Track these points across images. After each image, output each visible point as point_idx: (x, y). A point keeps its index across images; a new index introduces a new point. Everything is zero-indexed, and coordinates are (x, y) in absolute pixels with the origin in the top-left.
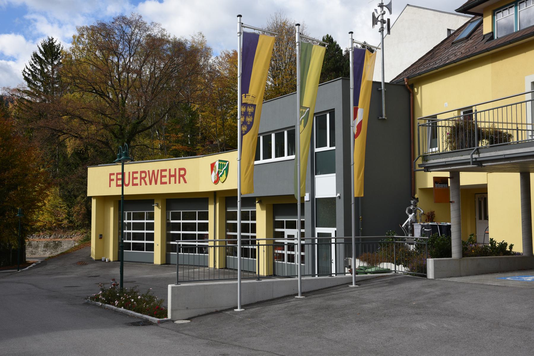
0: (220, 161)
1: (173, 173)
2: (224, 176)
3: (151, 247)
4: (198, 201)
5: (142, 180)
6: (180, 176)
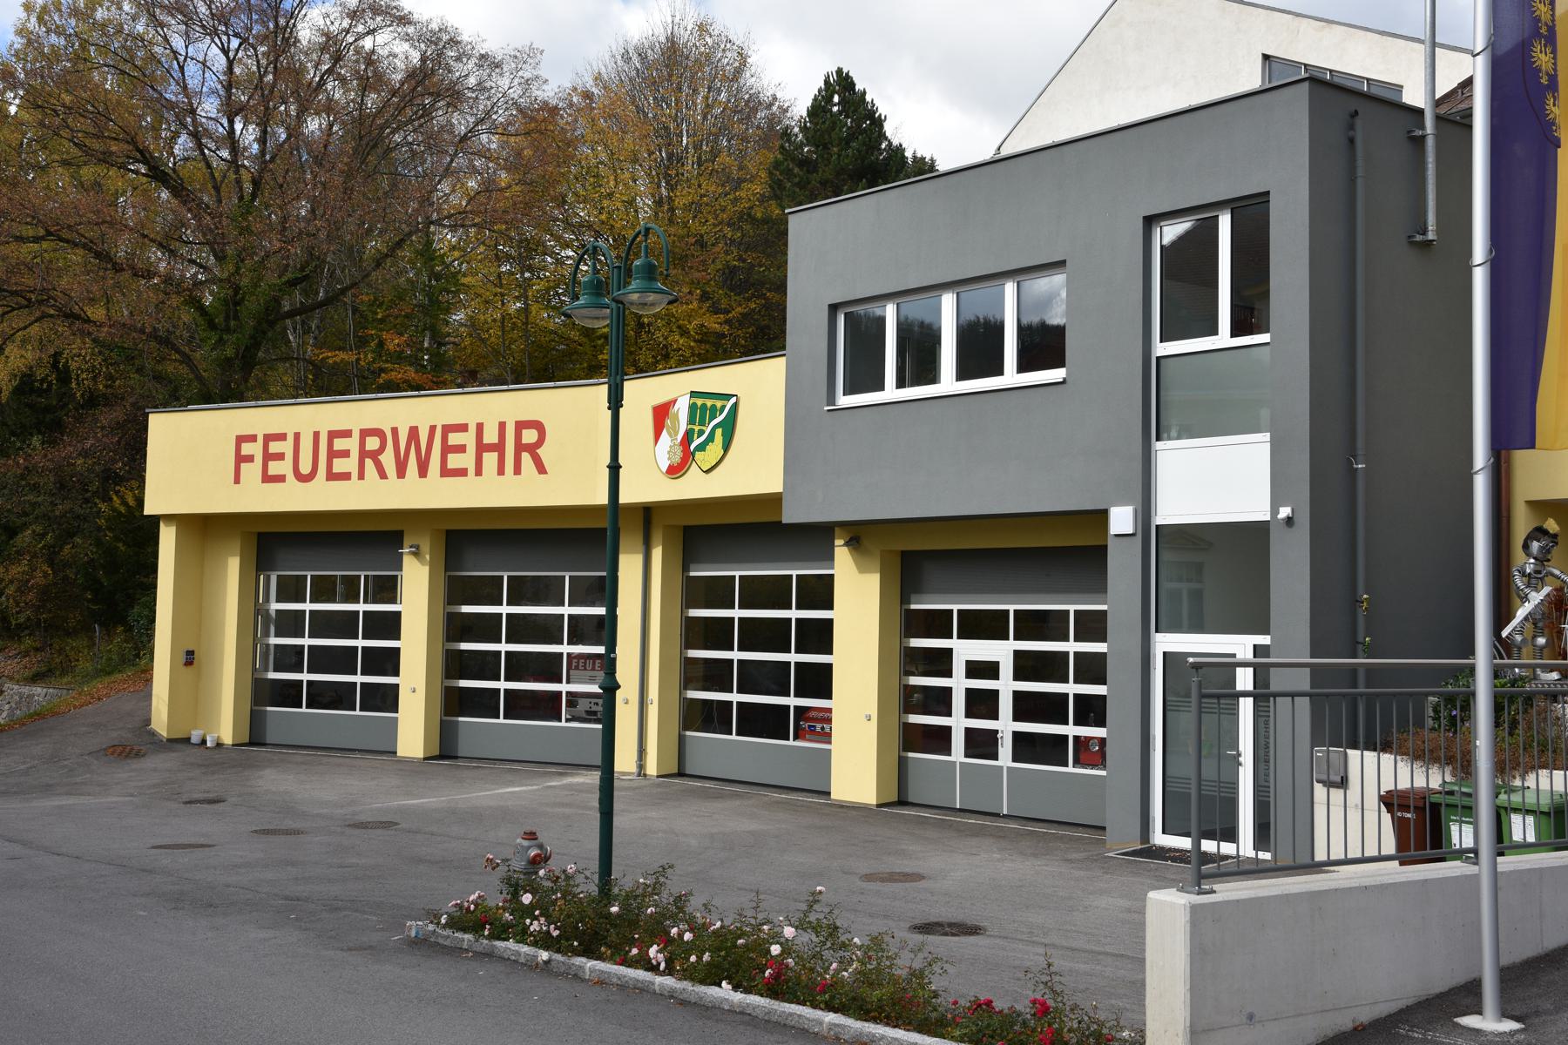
0: (693, 394)
1: (491, 437)
2: (715, 449)
3: (386, 699)
4: (582, 542)
5: (369, 463)
6: (520, 447)
